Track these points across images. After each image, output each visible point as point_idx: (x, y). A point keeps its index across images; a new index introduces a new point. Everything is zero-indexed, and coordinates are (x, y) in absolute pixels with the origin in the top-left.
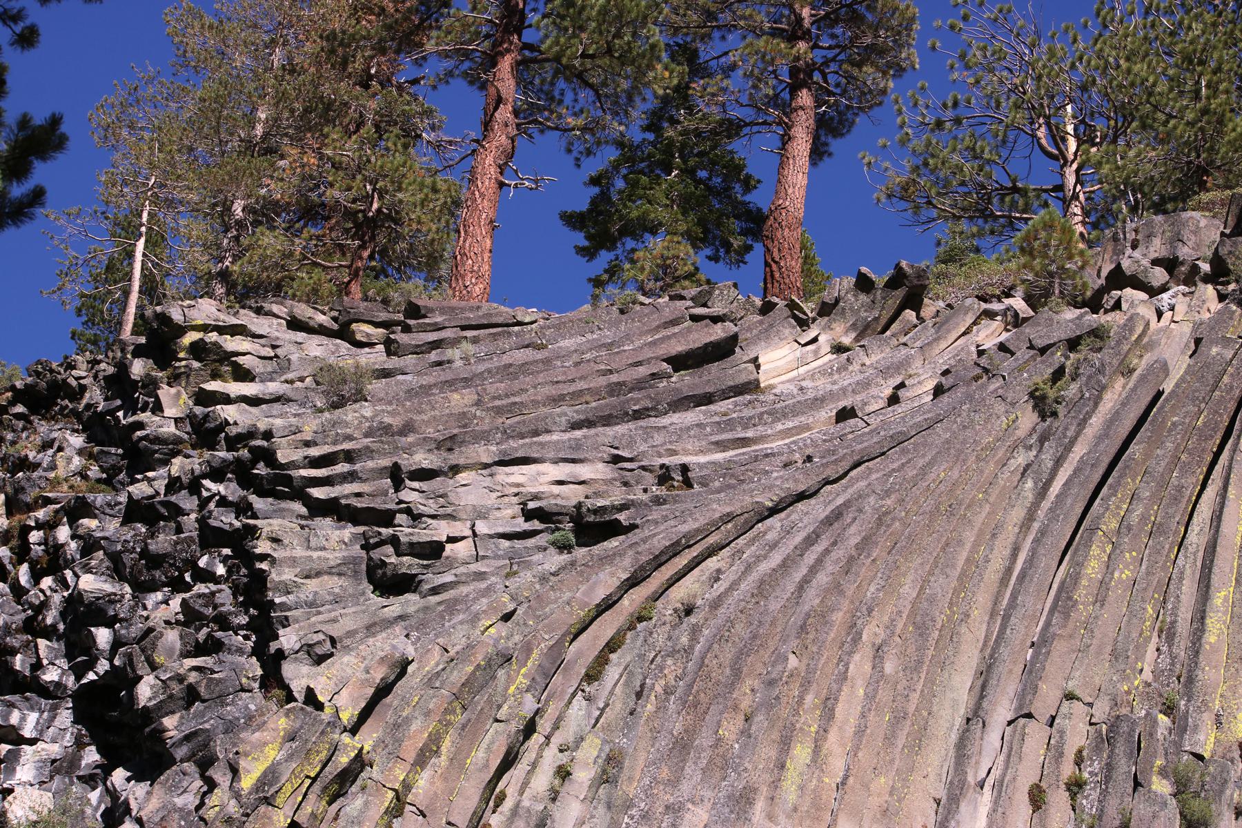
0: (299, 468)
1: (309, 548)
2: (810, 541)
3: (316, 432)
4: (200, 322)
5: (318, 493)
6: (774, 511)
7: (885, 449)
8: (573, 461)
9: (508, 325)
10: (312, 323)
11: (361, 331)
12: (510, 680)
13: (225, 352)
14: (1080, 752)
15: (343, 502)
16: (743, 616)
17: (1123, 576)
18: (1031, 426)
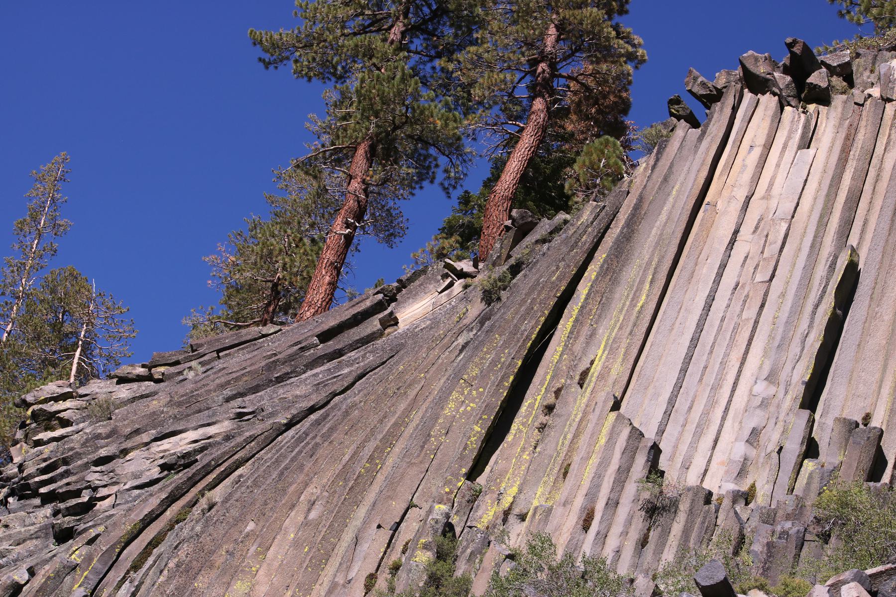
0: (35, 477)
1: (25, 526)
2: (300, 440)
3: (52, 452)
4: (43, 398)
5: (43, 490)
6: (289, 425)
7: (385, 359)
8: (209, 425)
9: (255, 339)
10: (130, 376)
11: (157, 372)
12: (74, 581)
13: (50, 413)
14: (407, 544)
15: (61, 491)
16: (238, 504)
17: (469, 408)
18: (478, 313)
